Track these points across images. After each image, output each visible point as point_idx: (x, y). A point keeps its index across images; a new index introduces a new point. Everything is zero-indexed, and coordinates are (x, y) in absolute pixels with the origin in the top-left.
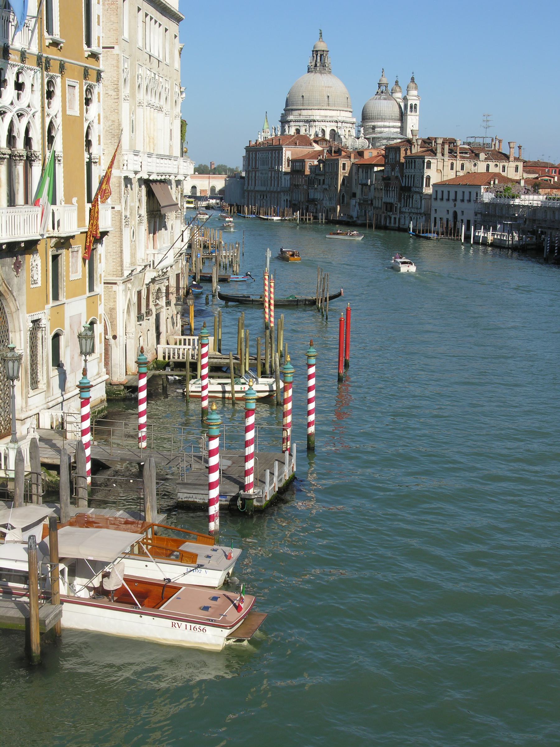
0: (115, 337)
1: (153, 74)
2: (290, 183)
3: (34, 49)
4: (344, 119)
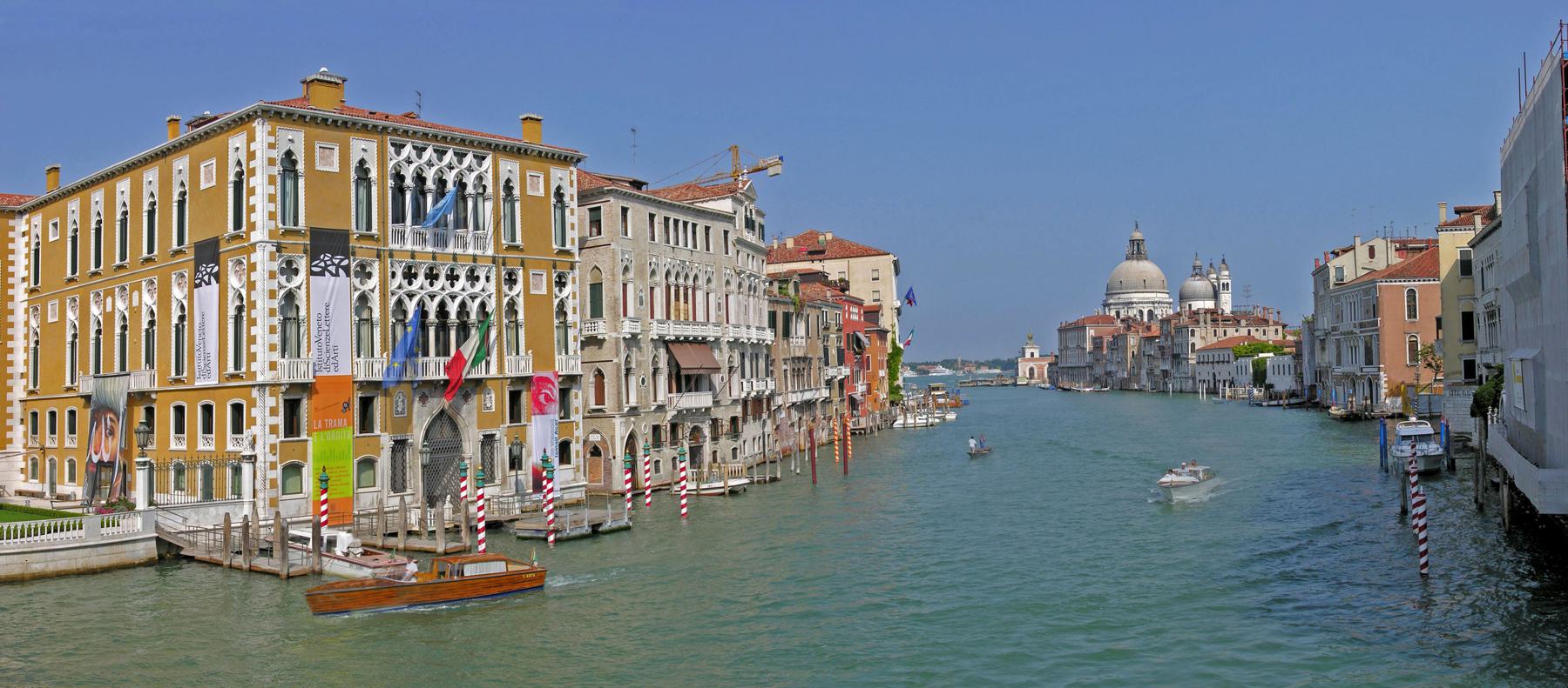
0: (614, 458)
1: (678, 262)
3: (490, 252)
4: (1161, 300)
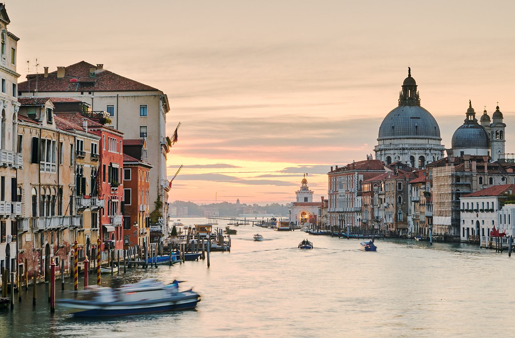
2: (362, 203)
